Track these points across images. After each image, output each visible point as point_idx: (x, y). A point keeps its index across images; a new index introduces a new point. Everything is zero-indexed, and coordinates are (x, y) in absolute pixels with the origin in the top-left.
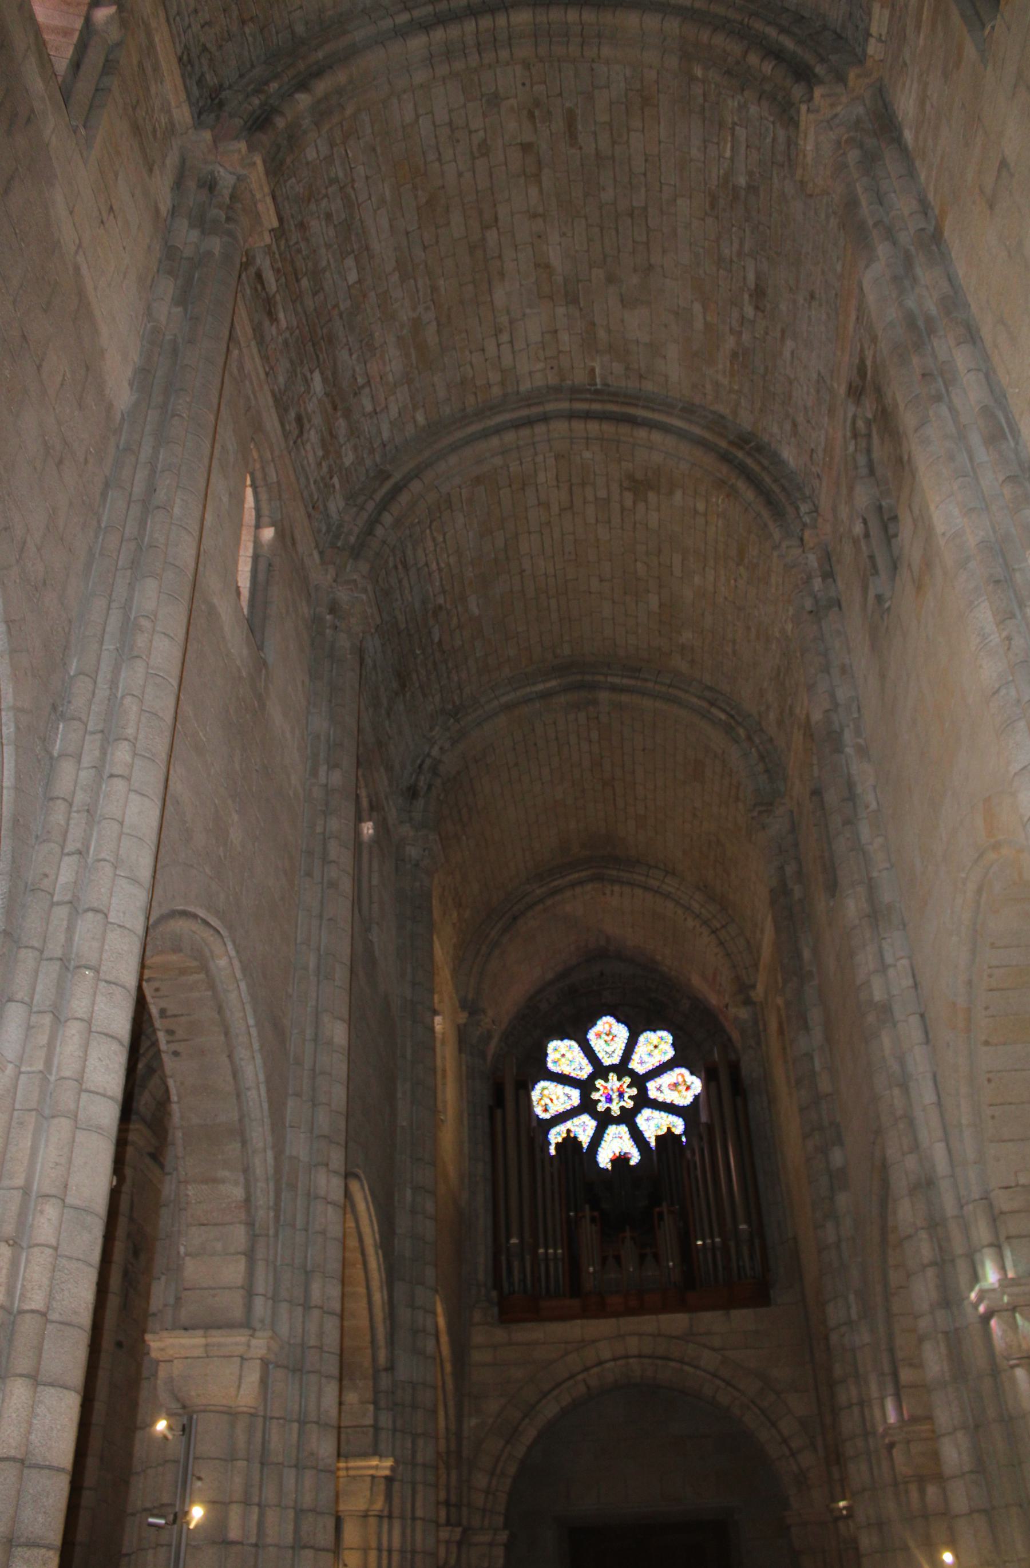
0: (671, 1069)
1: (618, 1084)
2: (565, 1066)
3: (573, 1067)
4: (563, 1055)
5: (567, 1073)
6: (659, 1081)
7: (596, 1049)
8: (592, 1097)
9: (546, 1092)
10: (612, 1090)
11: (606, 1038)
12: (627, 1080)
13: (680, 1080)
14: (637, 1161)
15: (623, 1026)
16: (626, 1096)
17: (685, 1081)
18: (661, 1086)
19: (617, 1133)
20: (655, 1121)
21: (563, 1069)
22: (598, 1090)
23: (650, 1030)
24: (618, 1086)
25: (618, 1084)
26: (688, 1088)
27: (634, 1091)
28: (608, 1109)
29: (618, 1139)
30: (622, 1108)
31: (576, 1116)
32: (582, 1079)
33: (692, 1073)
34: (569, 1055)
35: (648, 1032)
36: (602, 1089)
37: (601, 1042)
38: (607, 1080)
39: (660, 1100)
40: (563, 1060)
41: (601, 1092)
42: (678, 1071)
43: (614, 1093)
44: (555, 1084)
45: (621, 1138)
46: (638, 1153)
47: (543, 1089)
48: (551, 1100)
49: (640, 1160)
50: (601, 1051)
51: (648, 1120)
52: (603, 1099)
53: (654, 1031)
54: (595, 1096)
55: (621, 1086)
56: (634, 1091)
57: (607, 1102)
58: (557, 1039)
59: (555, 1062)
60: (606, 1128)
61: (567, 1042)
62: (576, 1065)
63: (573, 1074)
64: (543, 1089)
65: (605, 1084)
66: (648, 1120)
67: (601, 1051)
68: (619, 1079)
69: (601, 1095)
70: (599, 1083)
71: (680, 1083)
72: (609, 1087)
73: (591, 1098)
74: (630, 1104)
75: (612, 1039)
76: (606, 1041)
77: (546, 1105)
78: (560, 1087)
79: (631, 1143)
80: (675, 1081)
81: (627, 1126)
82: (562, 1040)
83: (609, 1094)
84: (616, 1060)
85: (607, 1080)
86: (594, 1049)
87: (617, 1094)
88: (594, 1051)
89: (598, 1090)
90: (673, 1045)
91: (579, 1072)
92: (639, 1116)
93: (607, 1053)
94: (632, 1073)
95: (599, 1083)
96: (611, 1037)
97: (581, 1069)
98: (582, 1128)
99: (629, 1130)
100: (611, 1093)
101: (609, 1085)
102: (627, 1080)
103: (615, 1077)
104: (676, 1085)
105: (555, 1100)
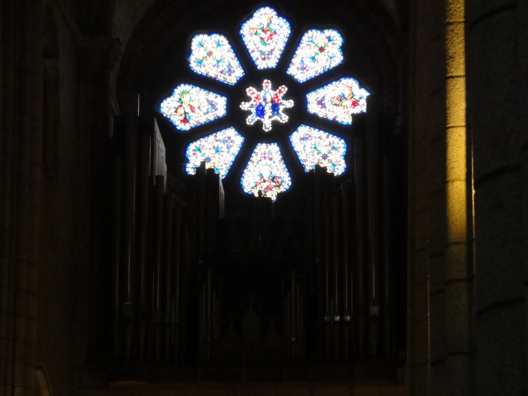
3: (221, 69)
12: (284, 89)
16: (281, 108)
20: (313, 141)
22: (248, 99)
25: (272, 93)
27: (290, 104)
28: (259, 124)
36: (253, 97)
37: (257, 39)
39: (321, 115)
41: (252, 102)
45: (271, 159)
52: (253, 110)
54: (244, 106)
61: (216, 37)
64: (184, 93)
65: (257, 93)
67: (256, 50)
68: (275, 88)
73: (241, 109)
74: (284, 119)
76: (262, 39)
79: (282, 166)
82: (210, 34)
83: (260, 105)
88: (247, 50)
96: (269, 33)
99: (281, 150)
100: (263, 104)
101: (262, 94)
102: (284, 89)
105: (197, 110)
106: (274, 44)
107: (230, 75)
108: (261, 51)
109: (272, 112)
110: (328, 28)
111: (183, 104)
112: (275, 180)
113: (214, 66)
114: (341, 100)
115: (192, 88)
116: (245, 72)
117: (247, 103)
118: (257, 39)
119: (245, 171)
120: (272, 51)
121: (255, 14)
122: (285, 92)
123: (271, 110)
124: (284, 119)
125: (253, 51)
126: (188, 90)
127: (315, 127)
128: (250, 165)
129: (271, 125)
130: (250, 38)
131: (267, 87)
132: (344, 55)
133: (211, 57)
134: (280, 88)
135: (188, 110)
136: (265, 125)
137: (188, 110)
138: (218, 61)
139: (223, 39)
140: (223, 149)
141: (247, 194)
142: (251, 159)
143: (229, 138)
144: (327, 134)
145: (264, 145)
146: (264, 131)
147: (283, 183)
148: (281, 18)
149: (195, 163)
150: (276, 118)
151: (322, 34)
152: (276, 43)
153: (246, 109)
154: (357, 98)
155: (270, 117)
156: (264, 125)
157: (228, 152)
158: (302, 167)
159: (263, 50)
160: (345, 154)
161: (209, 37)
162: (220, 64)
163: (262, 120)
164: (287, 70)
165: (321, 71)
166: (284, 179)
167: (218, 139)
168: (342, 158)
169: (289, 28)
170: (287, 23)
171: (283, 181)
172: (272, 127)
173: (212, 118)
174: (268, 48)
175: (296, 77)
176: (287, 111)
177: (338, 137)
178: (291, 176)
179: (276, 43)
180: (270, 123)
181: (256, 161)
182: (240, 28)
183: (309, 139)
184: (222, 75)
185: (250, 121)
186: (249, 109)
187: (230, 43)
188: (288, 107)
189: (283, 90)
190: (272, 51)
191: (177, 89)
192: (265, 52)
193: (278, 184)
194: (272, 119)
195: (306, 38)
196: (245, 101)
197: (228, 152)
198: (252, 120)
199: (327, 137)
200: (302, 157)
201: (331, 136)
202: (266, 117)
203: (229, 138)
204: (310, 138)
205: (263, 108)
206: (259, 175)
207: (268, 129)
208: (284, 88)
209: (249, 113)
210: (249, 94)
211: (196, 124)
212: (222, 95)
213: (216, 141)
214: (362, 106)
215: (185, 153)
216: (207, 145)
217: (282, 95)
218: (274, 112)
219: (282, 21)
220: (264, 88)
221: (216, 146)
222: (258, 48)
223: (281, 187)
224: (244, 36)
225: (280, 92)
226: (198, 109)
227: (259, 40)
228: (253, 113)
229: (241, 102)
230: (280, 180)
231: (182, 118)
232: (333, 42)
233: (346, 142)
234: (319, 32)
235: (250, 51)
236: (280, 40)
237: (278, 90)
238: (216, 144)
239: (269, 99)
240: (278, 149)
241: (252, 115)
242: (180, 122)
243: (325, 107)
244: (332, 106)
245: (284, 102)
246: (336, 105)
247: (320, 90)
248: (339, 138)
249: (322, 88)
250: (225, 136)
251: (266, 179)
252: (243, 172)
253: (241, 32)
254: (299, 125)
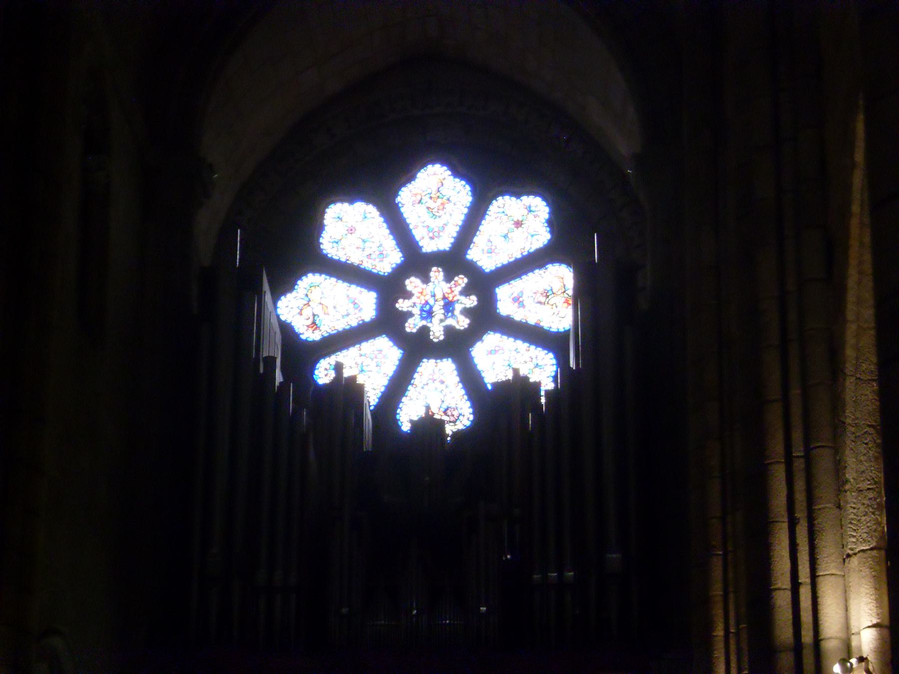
3: (367, 252)
8: (397, 306)
11: (431, 204)
12: (462, 281)
14: (468, 423)
16: (458, 308)
27: (472, 301)
28: (424, 331)
37: (421, 209)
38: (426, 279)
41: (414, 299)
43: (436, 301)
46: (471, 410)
52: (416, 311)
54: (402, 305)
56: (472, 301)
57: (423, 318)
62: (371, 248)
63: (367, 265)
70: (412, 283)
74: (462, 323)
83: (427, 303)
84: (444, 243)
85: (426, 279)
87: (442, 303)
92: (479, 345)
94: (471, 270)
95: (412, 283)
100: (431, 302)
101: (430, 288)
102: (462, 281)
105: (331, 310)
114: (547, 297)
119: (404, 399)
121: (419, 175)
122: (463, 285)
134: (456, 279)
153: (405, 309)
155: (442, 321)
156: (431, 333)
163: (429, 325)
164: (466, 254)
174: (439, 222)
176: (467, 312)
177: (544, 348)
180: (442, 329)
182: (396, 195)
184: (370, 261)
185: (412, 326)
186: (410, 309)
188: (468, 306)
189: (460, 281)
196: (404, 298)
202: (436, 320)
205: (431, 307)
207: (438, 338)
209: (410, 315)
212: (370, 289)
213: (361, 355)
217: (459, 289)
220: (432, 279)
230: (456, 413)
234: (514, 199)
238: (359, 360)
239: (439, 296)
245: (463, 299)
248: (546, 352)
252: (400, 402)
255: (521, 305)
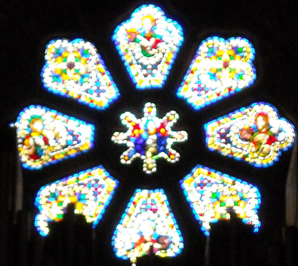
0: (248, 105)
1: (158, 122)
2: (72, 82)
3: (86, 86)
4: (71, 66)
5: (75, 96)
6: (225, 122)
7: (127, 59)
8: (113, 138)
9: (37, 126)
10: (147, 130)
12: (173, 116)
13: (261, 123)
15: (176, 23)
16: (170, 142)
17: (268, 127)
18: (228, 131)
19: (149, 202)
20: (214, 188)
21: (69, 88)
22: (124, 129)
23: (220, 36)
24: (158, 125)
25: (158, 122)
26: (272, 140)
27: (182, 136)
28: (138, 163)
29: (150, 213)
30: (161, 163)
31: (84, 170)
32: (98, 108)
33: (281, 115)
34: (80, 66)
35: (216, 38)
36: (130, 126)
37: (136, 48)
38: (139, 114)
39: (225, 153)
40: (70, 73)
41: (129, 133)
42: (258, 108)
43: (149, 135)
44: (53, 113)
45: (155, 211)
46: (181, 239)
47: (34, 119)
48: (46, 140)
49: (183, 250)
50: (134, 62)
51: (202, 185)
52: (131, 144)
53: (226, 37)
54: (118, 138)
55: (163, 126)
56: (182, 136)
57: (137, 151)
58: (61, 38)
59: (57, 77)
60: (132, 193)
61: (80, 43)
62: (90, 84)
63: (85, 99)
64: (34, 119)
65: (136, 121)
66: (202, 185)
67: (134, 62)
68: (161, 114)
69: (128, 139)
71: (260, 127)
72: (142, 126)
73: (112, 142)
74: (175, 157)
75: (155, 47)
76: (143, 49)
77: (37, 146)
78: (62, 118)
79: (171, 220)
80: (252, 125)
81: (166, 193)
82: (71, 39)
83: (140, 136)
85: (139, 114)
86: (123, 58)
87: (155, 137)
88: (123, 62)
89: (124, 129)
90: (255, 63)
91: (94, 96)
92: (188, 178)
93: (144, 67)
96: (153, 40)
97: (99, 92)
98: (93, 189)
99: (169, 199)
100: (144, 135)
101: (142, 122)
102: (173, 116)
103: (154, 110)
104: (253, 131)
105: (52, 142)
106: (161, 55)
107: (99, 95)
108: (141, 64)
109: (156, 147)
110: (236, 36)
111: (33, 134)
112: (161, 240)
113: (77, 82)
114: (253, 134)
115: (46, 112)
116: (120, 92)
117: (122, 133)
118: (136, 48)
119: (119, 227)
120: (159, 63)
121: (134, 14)
122: (175, 121)
123: (155, 145)
124: (175, 157)
125: (131, 64)
126: (39, 115)
127: (217, 170)
128: (125, 219)
129: (155, 165)
130: (127, 46)
131: (149, 113)
132: (257, 73)
133: (72, 70)
134: (168, 114)
135: (40, 141)
136: (148, 165)
137: (40, 141)
138: (83, 77)
139: (89, 46)
140: (87, 197)
141: (120, 259)
142: (126, 210)
143: (97, 181)
144: (233, 178)
145: (146, 192)
146: (145, 172)
147: (172, 246)
148: (170, 20)
149: (48, 214)
150: (163, 155)
151: (227, 43)
152: (164, 54)
153: (120, 142)
154: (274, 130)
155: (154, 154)
156: (144, 165)
157: (96, 200)
158: (198, 225)
159: (145, 63)
160: (258, 207)
161: (70, 43)
162: (85, 79)
163: (143, 157)
164: (176, 91)
165: (225, 93)
166: (173, 240)
167: (80, 182)
168: (254, 212)
169: (182, 33)
170: (179, 26)
171: (171, 242)
172: (157, 167)
173: (73, 153)
174: (153, 61)
175: (189, 101)
176: (177, 146)
177: (249, 183)
178: (183, 235)
179: (164, 54)
180: (154, 161)
181: (134, 214)
182: (112, 33)
183: (208, 185)
184: (88, 95)
185: (126, 158)
186: (125, 142)
187: (98, 52)
188: (179, 140)
189: (171, 117)
190: (159, 63)
191: (24, 112)
192: (147, 66)
193: (164, 246)
194: (156, 157)
195: (203, 48)
196: (120, 132)
197: (96, 200)
198: (130, 157)
199: (234, 184)
200: (197, 209)
201: (238, 182)
202: (149, 153)
203: (97, 181)
204: (209, 184)
205: (145, 141)
206: (138, 233)
207: (150, 170)
208: (174, 115)
209: (124, 148)
210: (124, 122)
211: (50, 160)
212: (88, 122)
213: (79, 184)
214: (282, 142)
215: (34, 200)
216: (65, 191)
217: (171, 124)
218: (160, 147)
219: (172, 24)
220: (146, 114)
221: (77, 191)
222: (137, 60)
223: (168, 250)
224: (119, 43)
225: (168, 120)
226: (54, 141)
227: (140, 49)
228: (130, 148)
229: (114, 132)
230: (166, 241)
231: (31, 151)
232: (242, 54)
233: (261, 191)
234: (222, 40)
235: (126, 64)
236: (168, 51)
237: (165, 118)
238: (78, 189)
239: (152, 130)
240: (164, 197)
241: (128, 150)
242: (28, 157)
243: (230, 142)
244: (240, 141)
245: (174, 134)
246: (246, 140)
247: (224, 118)
248: (251, 185)
249: (226, 116)
250: (91, 178)
251: (147, 238)
252: (114, 229)
253: (114, 37)
254: (194, 166)
255: (228, 141)
